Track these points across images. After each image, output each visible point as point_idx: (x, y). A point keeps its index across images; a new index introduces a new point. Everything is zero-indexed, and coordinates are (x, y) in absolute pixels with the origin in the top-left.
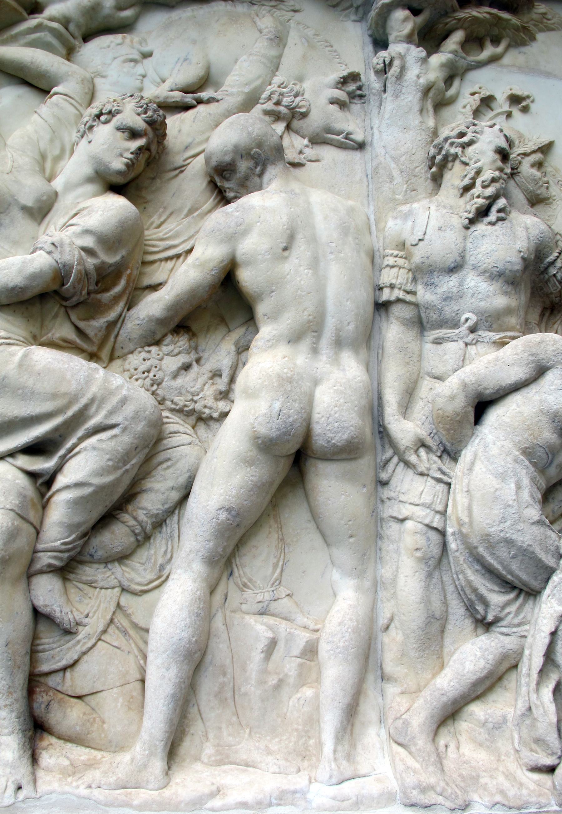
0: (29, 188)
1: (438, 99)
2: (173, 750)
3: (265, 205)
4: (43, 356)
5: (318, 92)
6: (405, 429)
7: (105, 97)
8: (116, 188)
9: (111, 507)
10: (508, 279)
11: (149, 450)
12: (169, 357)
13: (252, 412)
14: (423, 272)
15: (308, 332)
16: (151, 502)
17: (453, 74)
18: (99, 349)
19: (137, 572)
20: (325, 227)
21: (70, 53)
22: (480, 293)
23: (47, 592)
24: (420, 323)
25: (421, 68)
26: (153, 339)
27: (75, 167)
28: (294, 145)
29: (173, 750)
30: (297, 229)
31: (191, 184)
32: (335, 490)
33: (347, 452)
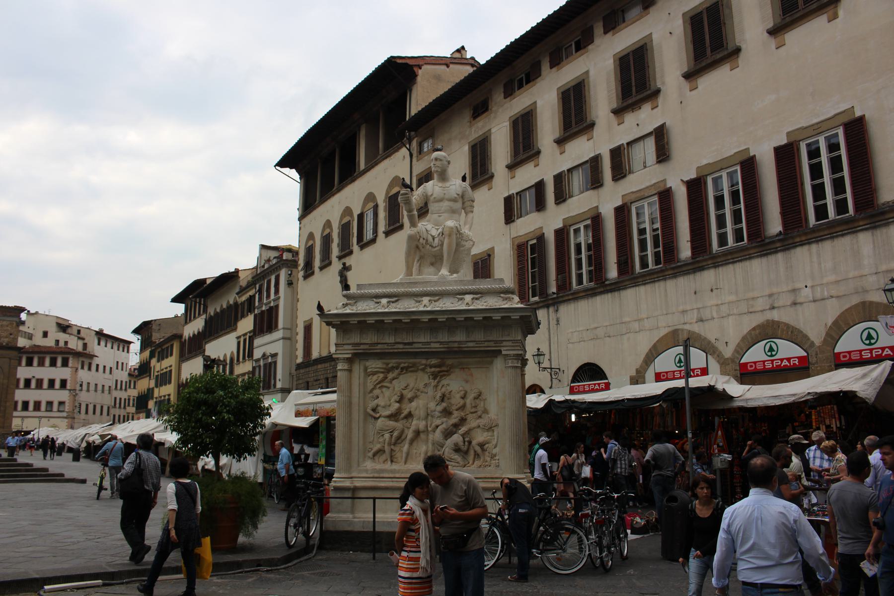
0: (388, 403)
1: (436, 386)
2: (405, 463)
3: (414, 404)
4: (391, 422)
5: (421, 386)
6: (430, 429)
7: (396, 389)
8: (398, 402)
9: (399, 438)
10: (441, 412)
11: (402, 432)
12: (405, 421)
13: (413, 428)
14: (432, 411)
15: (419, 419)
16: (403, 437)
17: (438, 382)
18: (397, 421)
19: (402, 445)
20: (421, 406)
21: (391, 382)
22: (437, 414)
23: (392, 447)
24: (432, 416)
25: (433, 383)
26: (403, 419)
27: (393, 400)
28: (419, 393)
29: (405, 463)
30: (416, 407)
31: (406, 401)
32: (422, 436)
33: (423, 432)
